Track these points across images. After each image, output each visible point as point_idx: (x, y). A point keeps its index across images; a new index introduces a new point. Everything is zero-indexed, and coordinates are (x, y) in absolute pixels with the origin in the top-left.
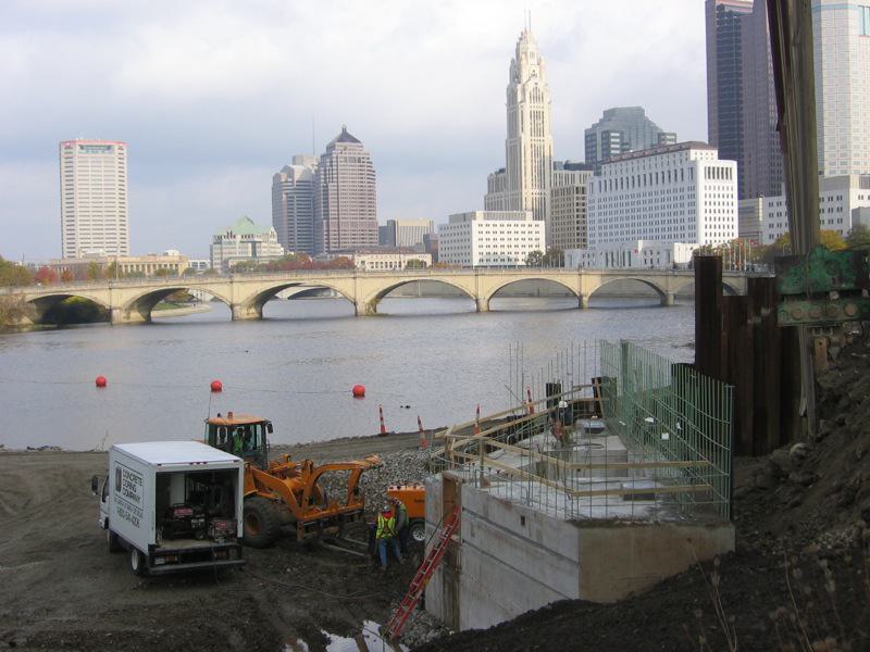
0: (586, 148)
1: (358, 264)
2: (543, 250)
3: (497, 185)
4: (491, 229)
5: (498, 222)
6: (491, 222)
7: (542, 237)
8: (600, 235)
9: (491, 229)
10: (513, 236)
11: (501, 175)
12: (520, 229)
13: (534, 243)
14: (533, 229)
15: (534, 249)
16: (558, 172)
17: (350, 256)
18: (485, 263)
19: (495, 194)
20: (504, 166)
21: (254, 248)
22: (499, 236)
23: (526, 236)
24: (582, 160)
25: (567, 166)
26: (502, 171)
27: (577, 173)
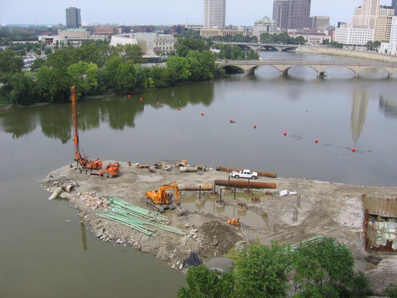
0: (392, 2)
1: (305, 39)
2: (373, 40)
3: (358, 13)
4: (355, 31)
5: (358, 29)
6: (355, 29)
7: (373, 35)
8: (395, 41)
9: (355, 31)
10: (362, 34)
11: (359, 9)
12: (365, 32)
13: (370, 37)
14: (370, 32)
15: (369, 40)
16: (381, 9)
17: (303, 36)
18: (351, 44)
19: (357, 16)
20: (361, 5)
21: (268, 28)
22: (357, 34)
23: (367, 34)
24: (390, 4)
25: (385, 7)
26: (360, 7)
27: (388, 10)
